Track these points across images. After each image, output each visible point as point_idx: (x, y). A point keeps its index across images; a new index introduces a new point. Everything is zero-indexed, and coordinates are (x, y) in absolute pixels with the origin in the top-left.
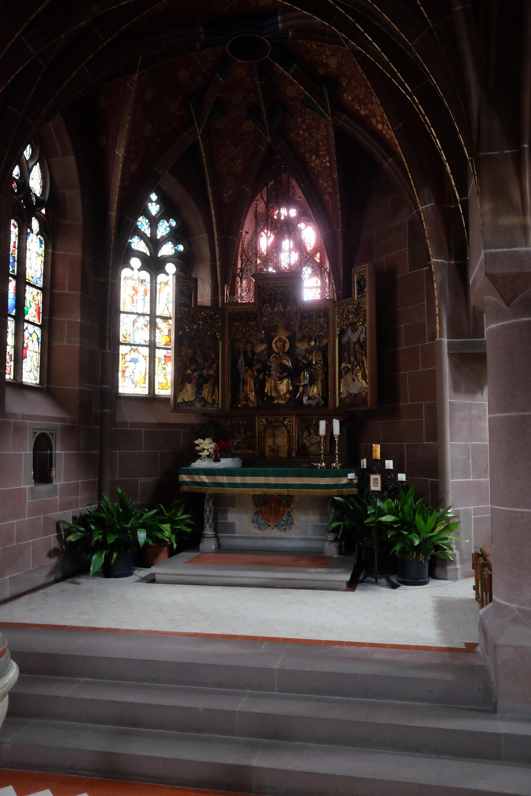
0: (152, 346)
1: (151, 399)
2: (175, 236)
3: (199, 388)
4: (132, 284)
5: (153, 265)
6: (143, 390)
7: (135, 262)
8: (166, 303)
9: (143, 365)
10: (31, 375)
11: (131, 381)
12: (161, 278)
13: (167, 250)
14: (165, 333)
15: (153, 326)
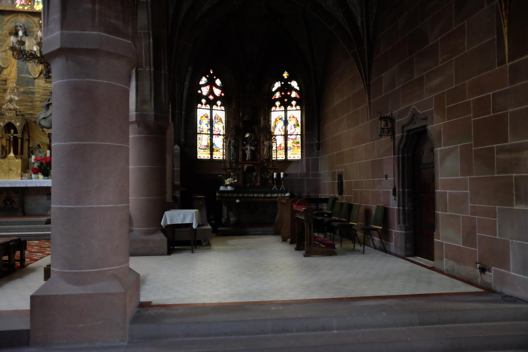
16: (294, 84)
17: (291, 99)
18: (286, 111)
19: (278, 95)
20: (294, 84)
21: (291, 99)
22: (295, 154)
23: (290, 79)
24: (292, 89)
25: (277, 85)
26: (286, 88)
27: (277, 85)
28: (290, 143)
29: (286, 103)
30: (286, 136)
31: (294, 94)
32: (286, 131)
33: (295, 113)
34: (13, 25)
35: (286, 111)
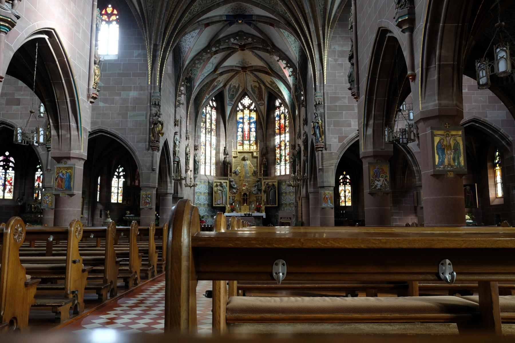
0: (118, 193)
1: (118, 203)
2: (123, 171)
3: (127, 201)
4: (115, 181)
5: (119, 177)
6: (116, 202)
7: (115, 177)
8: (121, 185)
9: (116, 197)
10: (98, 200)
11: (114, 200)
12: (120, 179)
13: (121, 174)
14: (120, 190)
15: (118, 189)
16: (348, 177)
17: (347, 182)
18: (345, 187)
19: (341, 181)
20: (348, 177)
21: (347, 182)
22: (349, 204)
23: (346, 174)
24: (347, 178)
25: (341, 177)
26: (345, 178)
27: (341, 177)
28: (347, 199)
29: (345, 184)
30: (345, 197)
31: (348, 181)
32: (345, 195)
33: (349, 188)
34: (243, 156)
35: (345, 187)
